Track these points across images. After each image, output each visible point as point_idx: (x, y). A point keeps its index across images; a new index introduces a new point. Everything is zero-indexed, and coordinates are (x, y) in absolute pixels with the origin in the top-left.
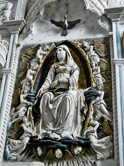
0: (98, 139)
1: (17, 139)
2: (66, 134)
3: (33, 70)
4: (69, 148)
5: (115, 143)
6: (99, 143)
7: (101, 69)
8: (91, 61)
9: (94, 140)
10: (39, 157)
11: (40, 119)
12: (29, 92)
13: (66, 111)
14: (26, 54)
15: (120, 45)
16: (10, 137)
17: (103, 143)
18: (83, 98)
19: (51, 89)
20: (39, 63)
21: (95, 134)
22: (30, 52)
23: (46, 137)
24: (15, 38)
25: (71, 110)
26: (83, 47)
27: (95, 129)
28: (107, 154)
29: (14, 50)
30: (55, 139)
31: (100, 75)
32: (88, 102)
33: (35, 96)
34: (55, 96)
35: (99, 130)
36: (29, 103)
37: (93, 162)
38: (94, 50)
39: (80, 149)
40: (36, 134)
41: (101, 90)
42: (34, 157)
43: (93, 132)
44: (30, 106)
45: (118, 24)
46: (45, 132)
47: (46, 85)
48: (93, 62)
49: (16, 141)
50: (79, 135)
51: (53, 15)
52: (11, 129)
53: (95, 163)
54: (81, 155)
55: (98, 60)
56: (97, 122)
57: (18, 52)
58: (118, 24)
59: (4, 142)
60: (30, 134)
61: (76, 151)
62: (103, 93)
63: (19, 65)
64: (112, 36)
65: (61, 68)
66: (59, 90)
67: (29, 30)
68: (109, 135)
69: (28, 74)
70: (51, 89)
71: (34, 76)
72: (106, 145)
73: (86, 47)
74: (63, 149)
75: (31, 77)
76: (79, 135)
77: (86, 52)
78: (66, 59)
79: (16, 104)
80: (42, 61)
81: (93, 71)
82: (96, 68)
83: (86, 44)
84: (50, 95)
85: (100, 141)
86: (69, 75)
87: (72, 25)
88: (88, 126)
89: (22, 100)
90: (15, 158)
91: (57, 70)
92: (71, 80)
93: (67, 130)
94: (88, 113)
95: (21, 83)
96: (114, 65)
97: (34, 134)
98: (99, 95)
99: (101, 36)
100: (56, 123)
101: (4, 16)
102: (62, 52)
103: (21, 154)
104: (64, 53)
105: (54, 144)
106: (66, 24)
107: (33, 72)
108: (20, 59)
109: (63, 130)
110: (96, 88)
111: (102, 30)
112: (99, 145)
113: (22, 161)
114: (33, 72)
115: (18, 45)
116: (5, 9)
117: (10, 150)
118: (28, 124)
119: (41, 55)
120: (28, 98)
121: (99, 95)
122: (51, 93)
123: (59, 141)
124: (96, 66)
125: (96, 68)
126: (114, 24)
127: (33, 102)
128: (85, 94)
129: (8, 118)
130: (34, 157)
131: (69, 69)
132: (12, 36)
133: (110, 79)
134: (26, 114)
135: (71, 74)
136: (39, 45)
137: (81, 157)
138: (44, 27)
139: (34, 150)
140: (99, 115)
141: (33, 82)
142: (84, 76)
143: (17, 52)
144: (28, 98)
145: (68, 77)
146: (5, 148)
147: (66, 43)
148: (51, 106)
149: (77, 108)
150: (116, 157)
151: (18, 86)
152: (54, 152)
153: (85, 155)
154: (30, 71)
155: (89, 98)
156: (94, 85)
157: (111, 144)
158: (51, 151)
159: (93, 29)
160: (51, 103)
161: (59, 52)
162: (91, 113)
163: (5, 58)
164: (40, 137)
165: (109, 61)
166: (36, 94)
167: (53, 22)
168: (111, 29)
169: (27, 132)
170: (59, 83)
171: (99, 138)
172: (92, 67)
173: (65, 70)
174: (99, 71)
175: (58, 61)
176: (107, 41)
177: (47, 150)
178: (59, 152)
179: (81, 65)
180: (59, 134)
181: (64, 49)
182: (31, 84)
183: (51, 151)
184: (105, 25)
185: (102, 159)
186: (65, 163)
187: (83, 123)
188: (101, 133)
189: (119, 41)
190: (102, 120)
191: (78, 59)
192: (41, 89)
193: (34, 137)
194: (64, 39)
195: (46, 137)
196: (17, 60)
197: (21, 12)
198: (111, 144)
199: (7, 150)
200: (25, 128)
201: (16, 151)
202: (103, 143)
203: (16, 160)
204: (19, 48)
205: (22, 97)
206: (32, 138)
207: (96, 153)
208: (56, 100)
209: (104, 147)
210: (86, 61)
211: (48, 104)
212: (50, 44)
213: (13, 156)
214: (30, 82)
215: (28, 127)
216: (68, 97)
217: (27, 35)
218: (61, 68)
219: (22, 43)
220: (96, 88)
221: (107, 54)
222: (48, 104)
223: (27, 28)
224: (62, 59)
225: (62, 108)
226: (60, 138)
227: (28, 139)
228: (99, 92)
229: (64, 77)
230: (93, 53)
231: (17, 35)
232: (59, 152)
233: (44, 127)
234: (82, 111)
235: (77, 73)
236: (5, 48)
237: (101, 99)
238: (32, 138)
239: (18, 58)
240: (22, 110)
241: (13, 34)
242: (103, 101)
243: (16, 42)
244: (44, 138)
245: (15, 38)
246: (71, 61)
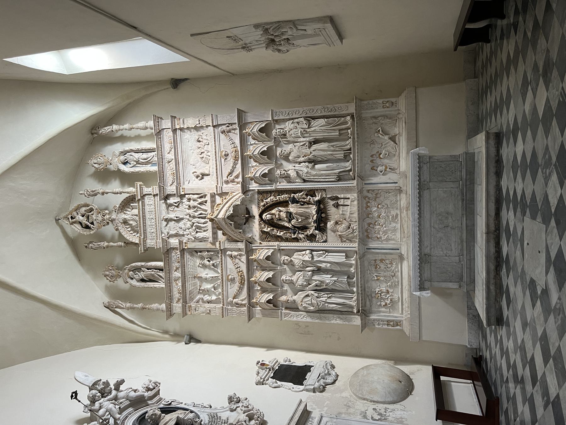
0: (316, 196)
1: (316, 237)
2: (314, 212)
3: (278, 232)
4: (321, 210)
5: (319, 189)
6: (318, 196)
7: (278, 196)
8: (273, 201)
9: (317, 198)
10: (325, 225)
11: (305, 226)
12: (290, 233)
13: (302, 213)
14: (265, 238)
15: (267, 186)
16: (315, 241)
17: (318, 195)
18: (295, 204)
19: (290, 222)
20: (273, 230)
21: (314, 198)
22: (264, 236)
23: (315, 222)
24: (254, 246)
25: (301, 210)
26: (264, 205)
27: (311, 198)
28: (324, 192)
29: (264, 245)
30: (317, 217)
31: (282, 196)
32: (297, 202)
33: (293, 230)
34: (294, 218)
35: (312, 197)
36: (297, 233)
37: (327, 199)
38: (266, 200)
39: (321, 205)
40: (314, 227)
41: (291, 195)
42: (325, 227)
43: (313, 199)
44: (298, 232)
45: (250, 186)
46: (312, 223)
47: (286, 224)
48: (274, 200)
49: (317, 237)
50: (315, 206)
51: (239, 225)
52: (311, 240)
53: (328, 198)
54: (324, 205)
55: (272, 197)
56: (308, 197)
57: (264, 243)
58: (250, 186)
59: (318, 243)
60: (313, 230)
61: (322, 207)
62: (292, 194)
63: (273, 241)
64: (258, 190)
65: (277, 217)
66: (291, 217)
67: (250, 238)
68: (314, 191)
69: (280, 235)
70: (290, 222)
71: (281, 232)
72: (320, 193)
73: (264, 204)
74: (322, 213)
75: (282, 233)
76: (315, 206)
77: (267, 204)
78: (273, 214)
79: (297, 240)
80: (272, 228)
81: (280, 200)
82: (278, 198)
83: (262, 204)
84: (293, 222)
85: (317, 196)
86: (281, 213)
87: (248, 212)
88: (310, 201)
89: (295, 236)
90: (325, 237)
91: (279, 218)
92: (285, 211)
93: (312, 212)
94: (303, 202)
95: (284, 238)
96: (277, 189)
97: (314, 228)
98: (294, 196)
99: (256, 196)
100: (307, 218)
101: (238, 255)
102: (266, 216)
103: (324, 234)
104: (268, 216)
105: (319, 218)
106: (247, 216)
107: (279, 232)
108: (269, 241)
109: (312, 213)
110: (289, 198)
111: (253, 195)
112: (320, 196)
113: (327, 233)
114: (279, 232)
115: (260, 243)
116: (231, 256)
117: (321, 240)
118: (308, 232)
119: (267, 229)
120: (294, 233)
121: (294, 196)
122: (292, 221)
123: (318, 215)
124: (276, 198)
125: (278, 198)
126: (251, 189)
127: (297, 230)
128: (293, 203)
129: (305, 243)
130: (325, 227)
131: (278, 213)
132: (253, 248)
133: (284, 191)
134: (303, 234)
135: (280, 211)
136: (262, 231)
137: (325, 204)
138: (247, 229)
139: (321, 228)
140: (304, 196)
141: (284, 232)
142: (281, 205)
143: (264, 243)
144: (294, 233)
145: (283, 213)
146: (321, 242)
147: (261, 215)
148: (300, 220)
149: (300, 208)
150: (326, 188)
151: (287, 240)
152: (323, 218)
153: (324, 203)
154: (278, 234)
155: (294, 201)
156: (288, 199)
157: (319, 190)
158: (322, 219)
159: (251, 201)
160: (298, 220)
161: (268, 218)
162: (303, 200)
163: (269, 250)
164: (316, 225)
165: (273, 191)
166: (292, 229)
167: (245, 224)
168: (253, 190)
169: (313, 232)
170: (286, 217)
171: (316, 196)
172: (277, 200)
173: (279, 215)
174: (280, 197)
175: (272, 219)
176: (260, 192)
177: (322, 221)
178: (323, 215)
179: (274, 206)
180: (314, 216)
181: (266, 216)
182: (286, 233)
183: (322, 219)
184: (250, 193)
185: (326, 195)
186: (328, 212)
187: (308, 204)
188: (313, 195)
189: (261, 186)
190: (307, 195)
191: (270, 208)
192: (290, 226)
193: (315, 228)
194: (257, 217)
195: (315, 222)
196: (269, 243)
197: (236, 245)
198: (319, 190)
199: (321, 241)
200: (311, 233)
201: (322, 237)
202: (318, 195)
203: (327, 236)
204: (262, 243)
205: (293, 237)
206: (315, 229)
207: (323, 197)
208: (296, 218)
209: (320, 194)
210: (273, 204)
211: (298, 222)
212: (260, 224)
213: (324, 239)
214: (284, 233)
215: (309, 232)
216: (295, 212)
217: (253, 239)
218: (277, 217)
219: (259, 241)
220: (289, 198)
221: (269, 193)
222: (298, 222)
223: (249, 239)
224: (272, 217)
225: (301, 215)
226: (316, 215)
227: (316, 231)
228: (292, 196)
229: (283, 215)
230: (269, 200)
231: (252, 245)
232: (323, 215)
233: (310, 223)
234: (302, 205)
235: (280, 208)
236: (262, 251)
237: (296, 196)
238: (315, 229)
239: (268, 243)
240: (301, 236)
241: (252, 248)
242: (297, 195)
243: (258, 245)
244: (316, 223)
245: (254, 246)
246: (273, 211)
